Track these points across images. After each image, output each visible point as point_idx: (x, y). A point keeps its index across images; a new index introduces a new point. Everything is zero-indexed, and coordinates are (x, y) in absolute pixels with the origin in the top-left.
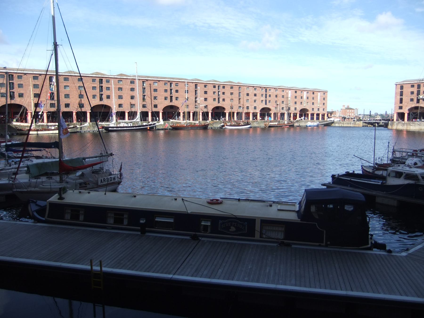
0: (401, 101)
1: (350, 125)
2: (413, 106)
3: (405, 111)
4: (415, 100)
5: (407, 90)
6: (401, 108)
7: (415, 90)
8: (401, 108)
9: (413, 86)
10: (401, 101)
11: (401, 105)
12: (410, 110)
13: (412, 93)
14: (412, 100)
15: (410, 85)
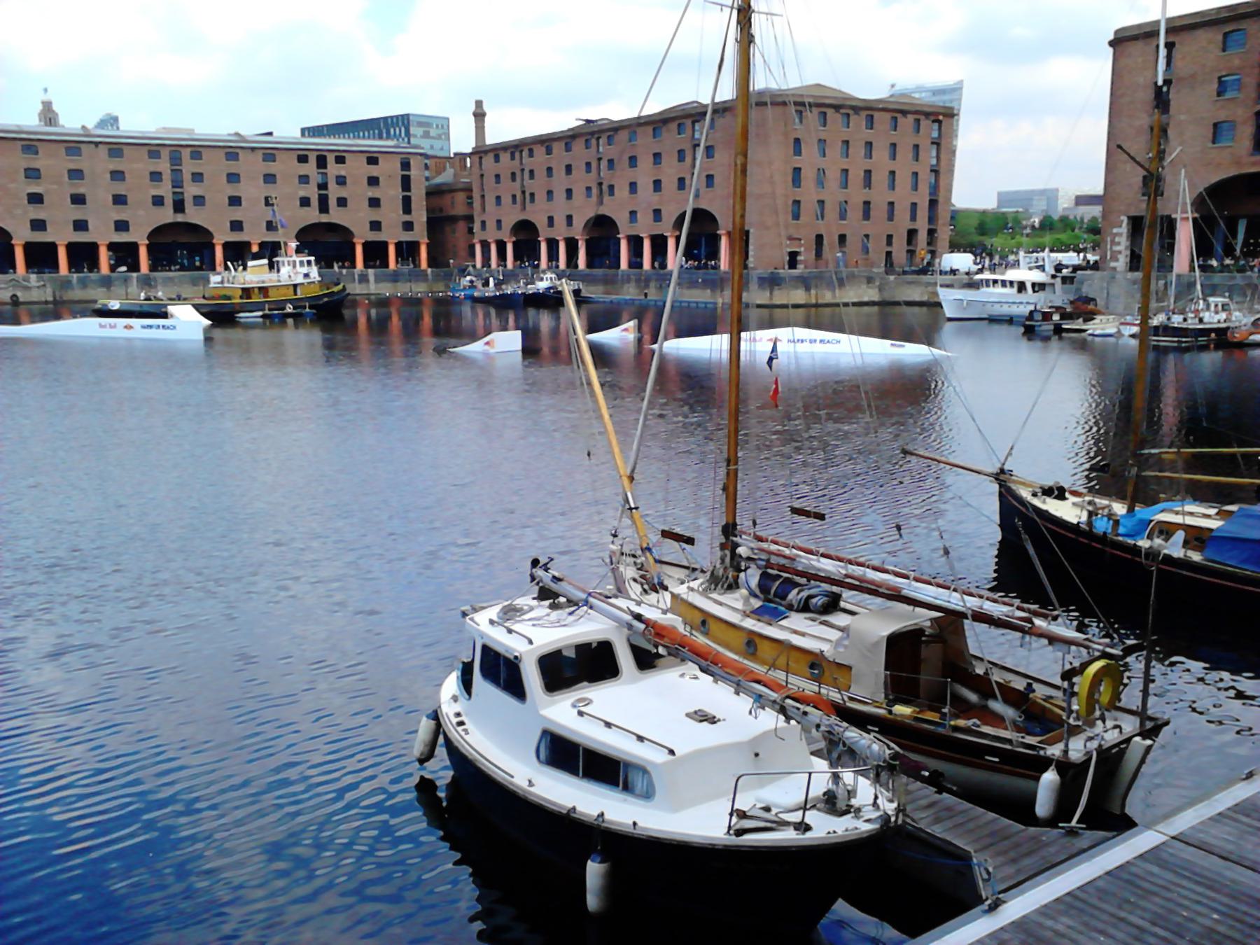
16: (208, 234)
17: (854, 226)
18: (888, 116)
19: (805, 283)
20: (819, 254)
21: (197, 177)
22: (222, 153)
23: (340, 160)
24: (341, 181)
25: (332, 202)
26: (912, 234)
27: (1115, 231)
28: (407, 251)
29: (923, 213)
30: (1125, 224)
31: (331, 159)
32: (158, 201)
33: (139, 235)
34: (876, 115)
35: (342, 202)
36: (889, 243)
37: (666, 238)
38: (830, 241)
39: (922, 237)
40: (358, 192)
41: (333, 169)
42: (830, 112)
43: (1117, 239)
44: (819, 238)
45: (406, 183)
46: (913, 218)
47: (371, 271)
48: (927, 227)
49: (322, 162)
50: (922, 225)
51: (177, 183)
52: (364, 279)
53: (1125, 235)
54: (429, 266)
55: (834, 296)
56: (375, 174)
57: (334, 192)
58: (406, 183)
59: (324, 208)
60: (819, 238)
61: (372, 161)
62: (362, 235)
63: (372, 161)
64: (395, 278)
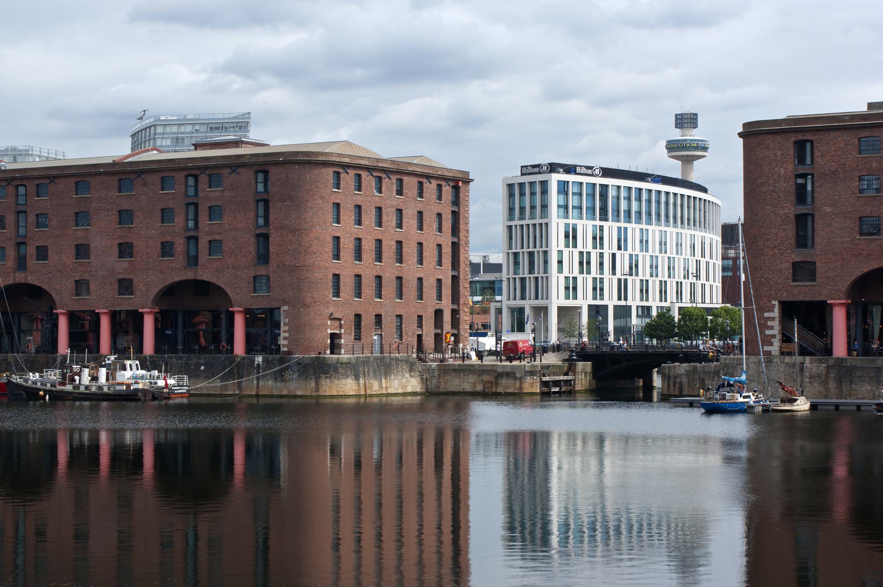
17: (389, 305)
18: (414, 181)
19: (355, 369)
20: (358, 337)
26: (439, 313)
27: (766, 315)
29: (447, 291)
30: (776, 310)
34: (406, 179)
36: (420, 325)
37: (141, 315)
38: (368, 321)
39: (447, 317)
42: (364, 174)
43: (770, 323)
44: (358, 317)
46: (440, 298)
48: (451, 306)
50: (446, 305)
53: (777, 319)
55: (381, 387)
60: (358, 317)
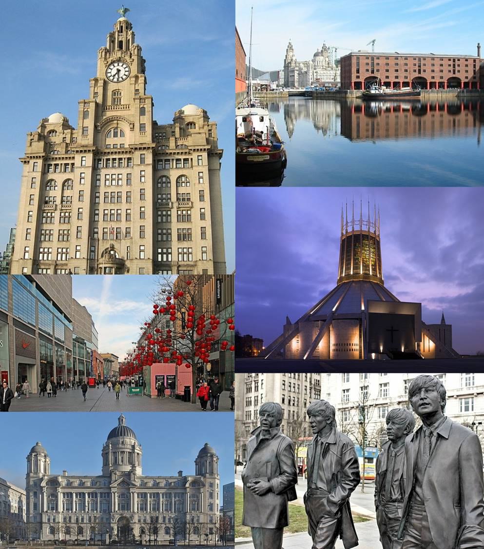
0: (358, 71)
1: (275, 95)
2: (368, 76)
3: (362, 80)
4: (370, 71)
5: (363, 61)
6: (358, 77)
7: (369, 61)
8: (358, 77)
9: (368, 58)
10: (358, 71)
11: (358, 75)
12: (366, 79)
13: (367, 64)
14: (367, 70)
15: (365, 57)
16: (426, 80)
21: (425, 65)
22: (384, 58)
23: (459, 60)
24: (459, 65)
25: (456, 71)
28: (474, 84)
31: (456, 60)
32: (415, 71)
33: (445, 80)
35: (459, 71)
40: (462, 68)
41: (457, 63)
45: (475, 66)
47: (465, 90)
49: (454, 61)
51: (420, 66)
52: (463, 92)
54: (480, 88)
56: (467, 64)
57: (457, 68)
58: (475, 66)
59: (454, 73)
61: (467, 60)
62: (463, 80)
63: (467, 60)
64: (471, 92)
